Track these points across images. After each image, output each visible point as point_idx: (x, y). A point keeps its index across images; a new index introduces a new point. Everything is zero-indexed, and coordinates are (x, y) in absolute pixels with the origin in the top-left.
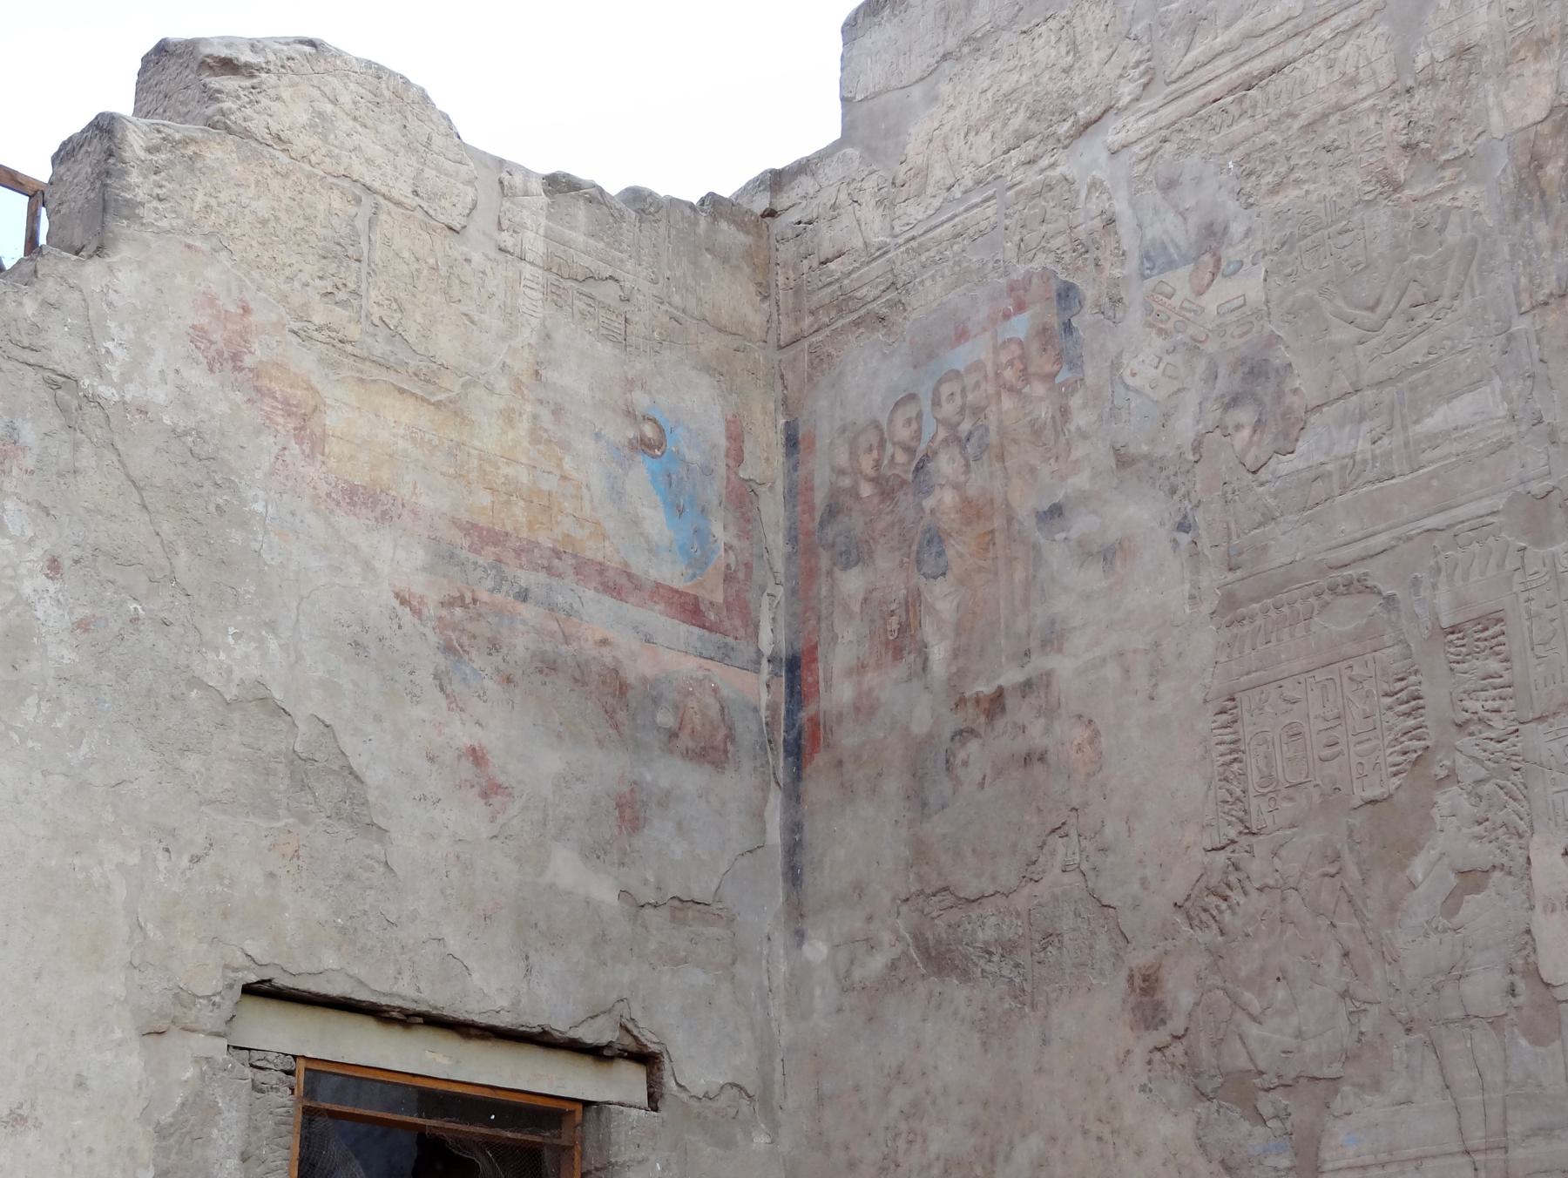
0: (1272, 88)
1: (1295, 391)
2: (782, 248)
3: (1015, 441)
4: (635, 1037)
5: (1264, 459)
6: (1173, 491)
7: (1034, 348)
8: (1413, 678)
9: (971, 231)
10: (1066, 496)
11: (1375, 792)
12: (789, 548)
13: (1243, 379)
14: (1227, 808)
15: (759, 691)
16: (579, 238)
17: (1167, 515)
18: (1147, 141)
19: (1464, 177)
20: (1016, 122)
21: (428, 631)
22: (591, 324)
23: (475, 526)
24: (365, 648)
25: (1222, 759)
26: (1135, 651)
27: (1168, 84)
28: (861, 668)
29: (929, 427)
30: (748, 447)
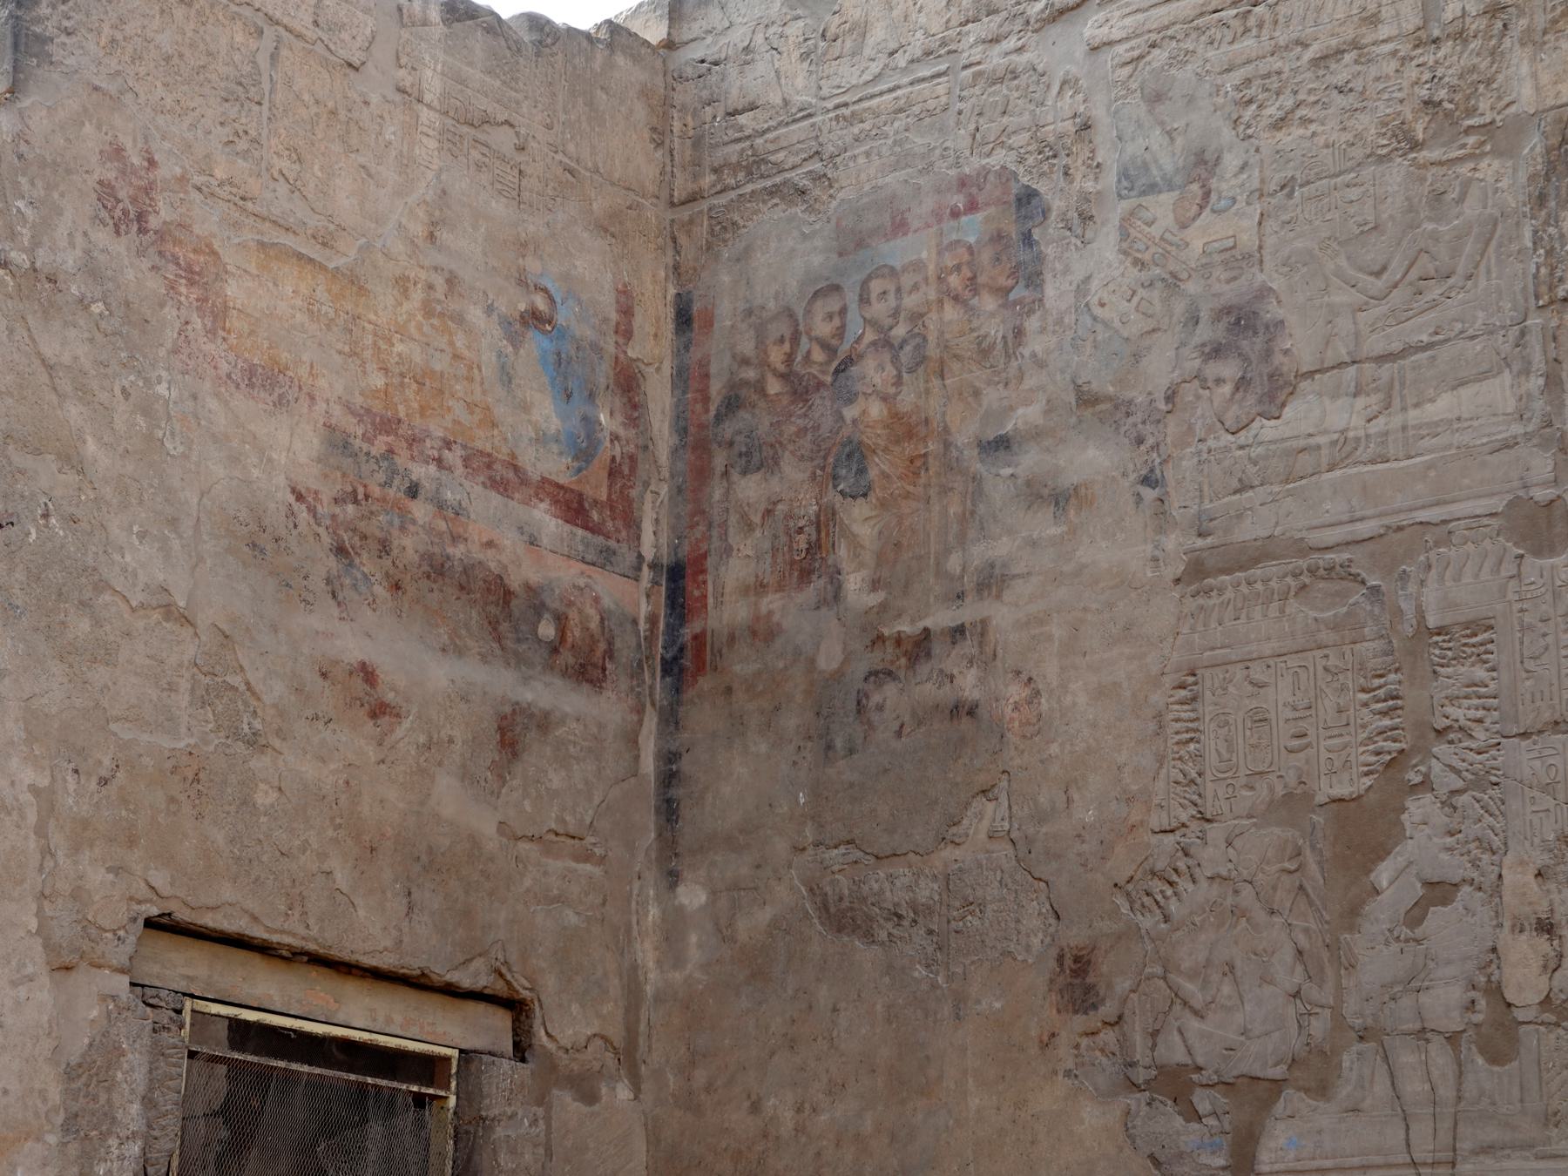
1: (1286, 352)
2: (679, 87)
4: (508, 983)
5: (1246, 421)
6: (1140, 441)
7: (986, 256)
8: (1392, 677)
9: (916, 109)
10: (1016, 429)
12: (675, 440)
13: (1228, 330)
14: (1179, 789)
15: (639, 600)
16: (475, 75)
17: (1131, 466)
18: (1133, 43)
19: (1488, 148)
21: (321, 530)
22: (484, 178)
23: (368, 411)
24: (262, 551)
25: (1178, 737)
28: (761, 587)
29: (855, 326)
30: (638, 321)
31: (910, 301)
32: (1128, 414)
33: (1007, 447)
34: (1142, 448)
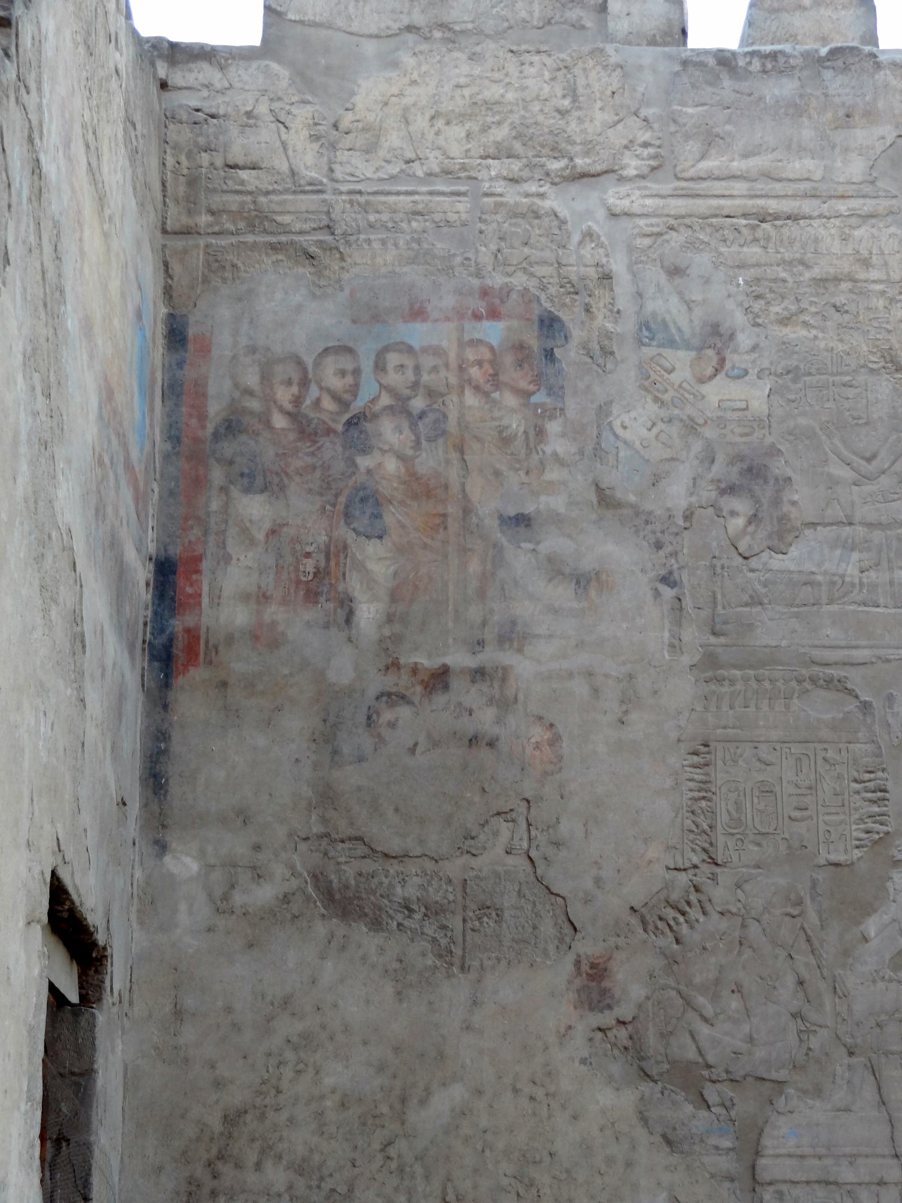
0: (785, 230)
1: (794, 503)
3: (478, 439)
5: (756, 549)
6: (659, 546)
7: (508, 360)
10: (538, 512)
11: (841, 858)
12: (168, 446)
13: (741, 473)
14: (692, 836)
17: (650, 565)
18: (654, 220)
20: (501, 134)
26: (606, 676)
27: (678, 179)
28: (263, 598)
29: (368, 389)
32: (647, 522)
33: (527, 526)
34: (661, 552)
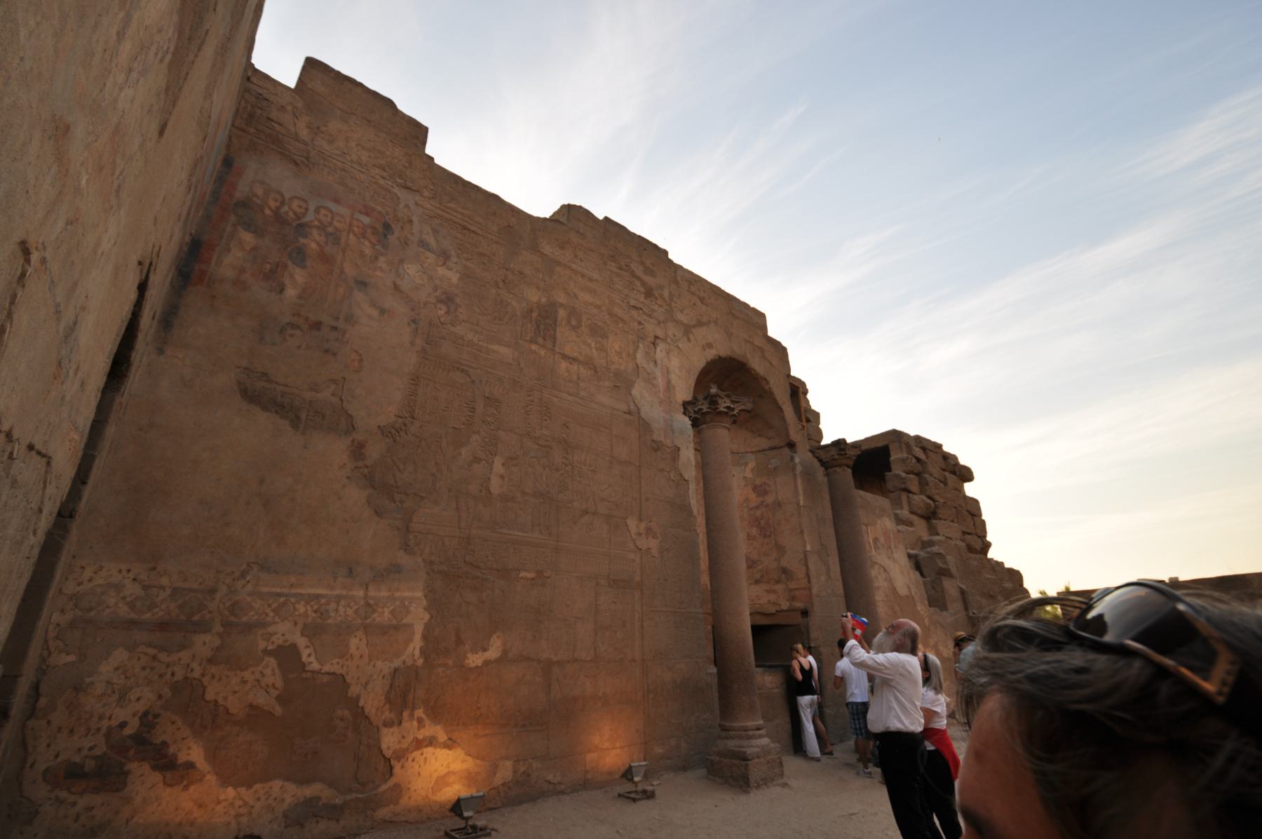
20: (382, 162)
29: (310, 217)
31: (336, 223)
